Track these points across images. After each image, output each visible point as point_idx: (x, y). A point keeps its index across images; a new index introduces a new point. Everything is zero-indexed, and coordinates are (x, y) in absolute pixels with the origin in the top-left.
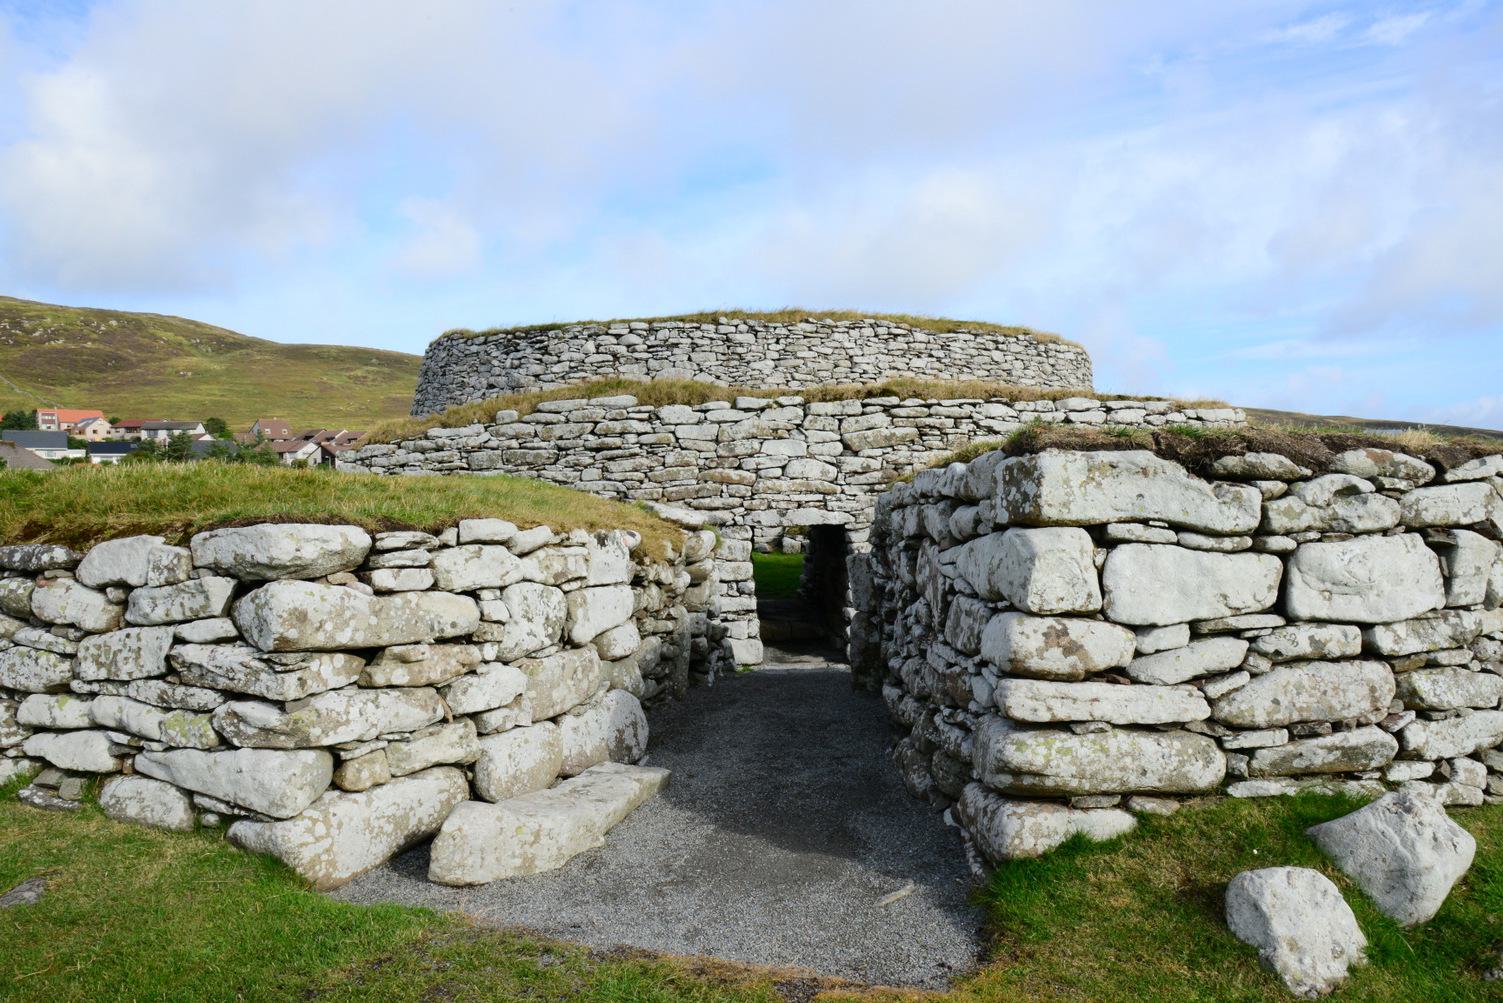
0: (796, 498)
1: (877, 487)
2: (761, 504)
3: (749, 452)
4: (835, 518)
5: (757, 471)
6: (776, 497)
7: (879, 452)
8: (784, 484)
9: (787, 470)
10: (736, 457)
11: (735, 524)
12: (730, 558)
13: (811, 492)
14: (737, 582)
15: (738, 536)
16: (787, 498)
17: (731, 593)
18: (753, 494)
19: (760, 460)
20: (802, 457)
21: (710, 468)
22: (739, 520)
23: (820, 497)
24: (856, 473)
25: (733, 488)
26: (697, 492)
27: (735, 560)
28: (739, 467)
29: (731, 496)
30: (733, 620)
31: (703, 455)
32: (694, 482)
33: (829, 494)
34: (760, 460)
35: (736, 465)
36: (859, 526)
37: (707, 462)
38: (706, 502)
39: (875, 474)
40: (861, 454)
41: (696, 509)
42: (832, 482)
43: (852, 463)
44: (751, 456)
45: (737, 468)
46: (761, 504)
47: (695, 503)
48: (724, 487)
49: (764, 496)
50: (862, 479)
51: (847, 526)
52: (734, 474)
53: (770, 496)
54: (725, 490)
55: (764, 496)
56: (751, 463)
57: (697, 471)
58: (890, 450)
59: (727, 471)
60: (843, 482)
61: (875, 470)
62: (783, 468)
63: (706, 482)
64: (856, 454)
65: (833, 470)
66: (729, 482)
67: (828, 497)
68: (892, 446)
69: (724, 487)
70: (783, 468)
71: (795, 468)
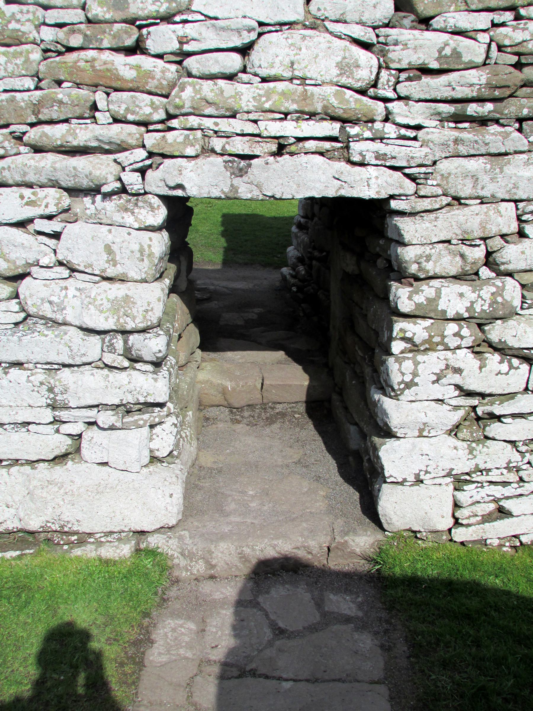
0: (275, 128)
1: (472, 109)
2: (187, 142)
4: (368, 184)
6: (225, 125)
7: (483, 20)
8: (246, 94)
9: (255, 55)
10: (131, 22)
11: (123, 190)
12: (110, 272)
13: (312, 115)
14: (125, 333)
15: (129, 219)
16: (250, 128)
17: (108, 359)
18: (170, 117)
20: (291, 24)
21: (70, 49)
22: (132, 179)
23: (332, 128)
24: (425, 71)
25: (121, 102)
26: (36, 108)
27: (122, 280)
28: (137, 49)
29: (116, 121)
30: (112, 428)
31: (52, 16)
32: (30, 83)
33: (354, 122)
34: (189, 30)
35: (129, 42)
36: (426, 204)
38: (57, 133)
40: (436, 23)
41: (37, 150)
42: (362, 92)
43: (417, 46)
44: (168, 19)
45: (130, 51)
46: (187, 142)
47: (33, 135)
49: (193, 121)
51: (394, 204)
52: (125, 66)
53: (208, 123)
55: (193, 121)
56: (163, 38)
57: (36, 56)
58: (508, 16)
59: (107, 56)
60: (391, 95)
62: (244, 50)
63: (59, 83)
64: (425, 22)
65: (367, 60)
67: (354, 130)
68: (512, 8)
70: (244, 50)
71: (272, 54)
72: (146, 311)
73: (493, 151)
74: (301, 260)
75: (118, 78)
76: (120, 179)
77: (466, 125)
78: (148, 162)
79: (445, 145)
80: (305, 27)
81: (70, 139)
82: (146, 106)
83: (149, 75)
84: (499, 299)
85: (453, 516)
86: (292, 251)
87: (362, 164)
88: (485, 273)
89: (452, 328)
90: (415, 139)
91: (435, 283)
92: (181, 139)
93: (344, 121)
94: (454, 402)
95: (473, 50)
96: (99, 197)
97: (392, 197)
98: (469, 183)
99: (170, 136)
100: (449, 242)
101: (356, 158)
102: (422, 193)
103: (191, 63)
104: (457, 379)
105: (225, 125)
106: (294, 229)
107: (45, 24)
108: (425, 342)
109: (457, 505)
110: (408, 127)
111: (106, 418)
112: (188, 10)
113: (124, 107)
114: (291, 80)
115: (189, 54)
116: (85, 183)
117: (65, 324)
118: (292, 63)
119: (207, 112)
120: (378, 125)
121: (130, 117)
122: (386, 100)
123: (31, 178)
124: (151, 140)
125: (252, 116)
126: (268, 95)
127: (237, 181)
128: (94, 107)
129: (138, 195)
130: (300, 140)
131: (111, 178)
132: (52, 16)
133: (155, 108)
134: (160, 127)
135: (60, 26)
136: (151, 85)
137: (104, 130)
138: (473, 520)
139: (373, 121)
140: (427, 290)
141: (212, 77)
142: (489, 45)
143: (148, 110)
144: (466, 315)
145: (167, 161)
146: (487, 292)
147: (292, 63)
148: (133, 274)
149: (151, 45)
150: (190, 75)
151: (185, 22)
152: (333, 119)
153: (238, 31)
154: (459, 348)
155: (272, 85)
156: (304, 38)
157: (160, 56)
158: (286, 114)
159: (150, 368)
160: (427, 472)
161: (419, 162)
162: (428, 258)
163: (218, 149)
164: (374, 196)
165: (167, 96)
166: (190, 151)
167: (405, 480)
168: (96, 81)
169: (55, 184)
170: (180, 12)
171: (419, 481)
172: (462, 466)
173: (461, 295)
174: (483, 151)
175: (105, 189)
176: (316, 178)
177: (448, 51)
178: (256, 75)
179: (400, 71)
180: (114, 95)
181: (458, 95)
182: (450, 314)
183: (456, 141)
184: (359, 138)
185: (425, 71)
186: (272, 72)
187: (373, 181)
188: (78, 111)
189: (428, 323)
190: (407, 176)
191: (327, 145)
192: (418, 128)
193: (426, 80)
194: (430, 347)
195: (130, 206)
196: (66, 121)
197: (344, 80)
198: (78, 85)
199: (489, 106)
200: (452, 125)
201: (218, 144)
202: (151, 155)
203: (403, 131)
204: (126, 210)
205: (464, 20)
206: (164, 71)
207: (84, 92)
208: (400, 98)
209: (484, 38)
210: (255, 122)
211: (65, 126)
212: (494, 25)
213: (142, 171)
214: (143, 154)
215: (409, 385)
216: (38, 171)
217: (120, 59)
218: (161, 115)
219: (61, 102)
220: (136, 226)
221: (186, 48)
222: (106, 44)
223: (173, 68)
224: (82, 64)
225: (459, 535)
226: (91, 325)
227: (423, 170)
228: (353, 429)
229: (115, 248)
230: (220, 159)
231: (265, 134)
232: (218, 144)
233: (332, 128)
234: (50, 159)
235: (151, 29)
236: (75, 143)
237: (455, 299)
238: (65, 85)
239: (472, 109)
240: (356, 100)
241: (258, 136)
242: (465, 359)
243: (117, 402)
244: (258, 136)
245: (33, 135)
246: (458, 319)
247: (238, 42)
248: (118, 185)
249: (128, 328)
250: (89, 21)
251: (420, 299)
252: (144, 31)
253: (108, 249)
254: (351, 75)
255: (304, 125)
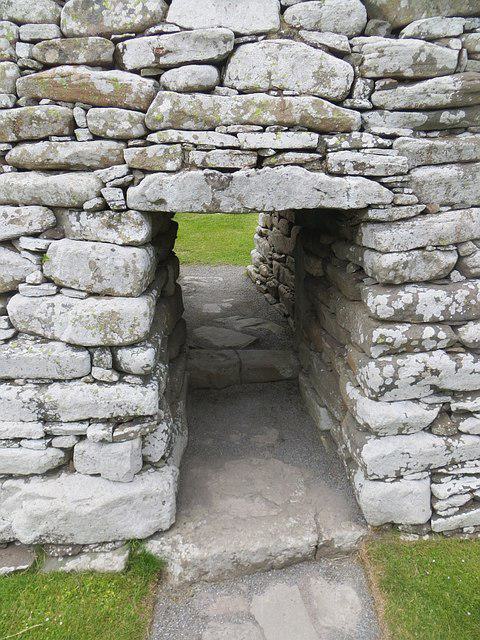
0: (255, 140)
1: (445, 117)
3: (137, 19)
4: (350, 193)
5: (156, 72)
6: (204, 138)
7: (456, 25)
8: (226, 104)
9: (231, 69)
10: (107, 36)
11: (105, 207)
12: (97, 288)
13: (291, 127)
14: (113, 349)
15: (112, 235)
16: (230, 141)
17: (97, 373)
19: (164, 41)
20: (266, 35)
21: (47, 66)
22: (113, 195)
23: (311, 140)
25: (98, 117)
26: (15, 125)
27: (109, 294)
28: (116, 63)
29: (96, 137)
31: (26, 31)
33: (331, 134)
34: (164, 41)
35: (107, 56)
36: (403, 212)
37: (36, 49)
38: (35, 151)
39: (447, 81)
40: (408, 31)
41: (20, 168)
42: (338, 102)
44: (139, 32)
45: (107, 66)
46: (167, 156)
48: (78, 112)
49: (173, 135)
50: (405, 94)
51: (371, 214)
52: (102, 81)
53: (188, 136)
54: (80, 121)
55: (173, 135)
56: (137, 52)
59: (83, 70)
60: (366, 104)
61: (444, 73)
63: (36, 101)
64: (395, 32)
65: (342, 67)
66: (92, 100)
67: (332, 141)
69: (78, 112)
70: (221, 64)
71: (249, 65)
72: (133, 326)
73: (465, 158)
74: (263, 260)
75: (99, 94)
76: (100, 195)
77: (436, 134)
78: (129, 178)
79: (419, 153)
80: (282, 36)
81: (51, 156)
82: (124, 121)
83: (127, 88)
84: (473, 302)
85: (432, 508)
86: (255, 254)
87: (341, 175)
88: (456, 276)
89: (429, 331)
90: (391, 147)
91: (410, 288)
92: (161, 153)
93: (322, 133)
94: (430, 400)
95: (447, 55)
96: (83, 215)
97: (370, 207)
98: (442, 190)
99: (150, 150)
100: (423, 248)
101: (336, 169)
102: (399, 202)
103: (166, 77)
104: (435, 380)
105: (204, 138)
106: (256, 236)
107: (20, 40)
108: (403, 345)
109: (433, 498)
110: (383, 136)
111: (96, 431)
112: (163, 21)
113: (103, 122)
114: (268, 92)
115: (167, 68)
116: (67, 201)
117: (54, 340)
118: (270, 74)
119: (186, 125)
120: (356, 135)
121: (110, 133)
122: (362, 110)
123: (15, 197)
124: (130, 154)
125: (230, 129)
126: (246, 107)
127: (220, 195)
128: (73, 125)
129: (120, 211)
130: (279, 151)
131: (92, 194)
132: (26, 31)
133: (133, 123)
134: (139, 142)
135: (34, 42)
136: (130, 99)
137: (83, 147)
138: (451, 511)
139: (350, 131)
140: (406, 296)
141: (189, 90)
142: (461, 51)
143: (126, 125)
144: (442, 318)
145: (149, 177)
146: (461, 294)
147: (270, 74)
148: (118, 289)
149: (129, 60)
150: (166, 89)
151: (160, 33)
152: (310, 130)
153: (215, 42)
154: (434, 349)
155: (250, 96)
156: (281, 46)
157: (136, 71)
158: (265, 127)
159: (138, 380)
160: (407, 469)
161: (398, 170)
162: (406, 264)
163: (198, 162)
164: (353, 205)
165: (145, 112)
166: (170, 166)
167: (386, 477)
168: (74, 97)
169: (39, 203)
170: (154, 25)
171: (399, 477)
172: (439, 461)
173: (437, 300)
174: (455, 158)
175: (87, 206)
176: (303, 189)
177: (423, 58)
178: (233, 88)
179: (375, 79)
180: (92, 111)
181: (428, 102)
182: (427, 318)
183: (431, 149)
184: (338, 149)
185: (402, 80)
186: (251, 83)
187: (351, 192)
188: (58, 127)
189: (406, 328)
190: (382, 184)
191: (306, 156)
192: (393, 137)
193: (401, 88)
194: (407, 349)
195: (113, 222)
196: (46, 139)
197: (321, 90)
198: (55, 102)
199: (462, 114)
200: (422, 134)
201: (196, 156)
202: (131, 170)
203: (381, 141)
204: (110, 226)
205: (438, 26)
206: (141, 85)
207: (62, 109)
208: (375, 108)
209: (456, 44)
210: (235, 134)
211: (46, 144)
212: (466, 31)
213: (124, 188)
214: (122, 169)
215: (392, 387)
216: (20, 189)
217: (96, 75)
218: (137, 131)
219: (39, 119)
220: (121, 242)
221: (163, 61)
222: (82, 59)
223: (151, 82)
224: (58, 80)
225: (439, 524)
226: (79, 341)
227: (400, 178)
228: (323, 411)
229: (99, 264)
230: (201, 173)
231: (245, 146)
232: (196, 156)
233: (310, 139)
234: (33, 179)
235: (126, 42)
236: (56, 160)
237: (430, 301)
238: (43, 102)
239: (445, 117)
240: (334, 110)
241: (238, 148)
242: (440, 360)
243: (108, 416)
244: (238, 148)
245: (15, 153)
246: (434, 322)
247: (213, 54)
248: (99, 201)
249: (116, 342)
250: (63, 36)
251: (399, 305)
252: (120, 45)
253: (93, 266)
254: (327, 84)
255: (282, 135)
